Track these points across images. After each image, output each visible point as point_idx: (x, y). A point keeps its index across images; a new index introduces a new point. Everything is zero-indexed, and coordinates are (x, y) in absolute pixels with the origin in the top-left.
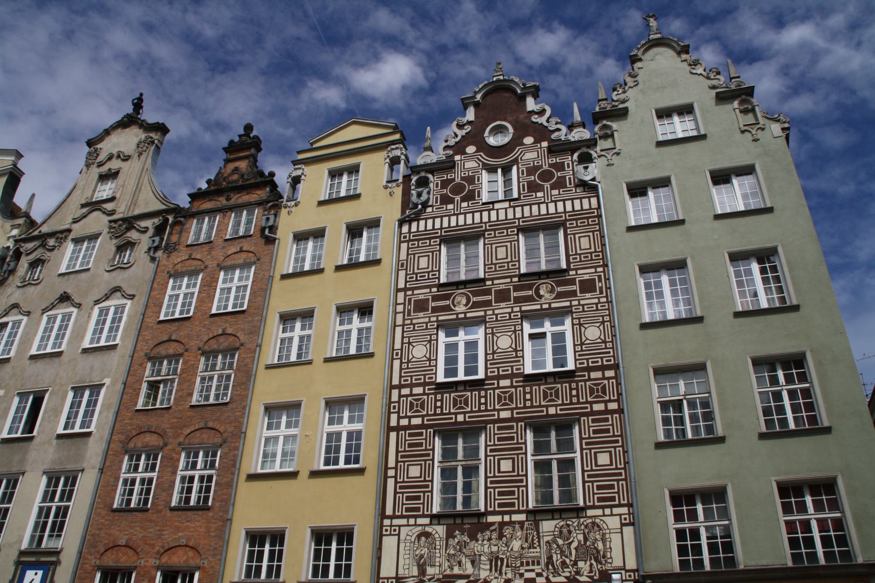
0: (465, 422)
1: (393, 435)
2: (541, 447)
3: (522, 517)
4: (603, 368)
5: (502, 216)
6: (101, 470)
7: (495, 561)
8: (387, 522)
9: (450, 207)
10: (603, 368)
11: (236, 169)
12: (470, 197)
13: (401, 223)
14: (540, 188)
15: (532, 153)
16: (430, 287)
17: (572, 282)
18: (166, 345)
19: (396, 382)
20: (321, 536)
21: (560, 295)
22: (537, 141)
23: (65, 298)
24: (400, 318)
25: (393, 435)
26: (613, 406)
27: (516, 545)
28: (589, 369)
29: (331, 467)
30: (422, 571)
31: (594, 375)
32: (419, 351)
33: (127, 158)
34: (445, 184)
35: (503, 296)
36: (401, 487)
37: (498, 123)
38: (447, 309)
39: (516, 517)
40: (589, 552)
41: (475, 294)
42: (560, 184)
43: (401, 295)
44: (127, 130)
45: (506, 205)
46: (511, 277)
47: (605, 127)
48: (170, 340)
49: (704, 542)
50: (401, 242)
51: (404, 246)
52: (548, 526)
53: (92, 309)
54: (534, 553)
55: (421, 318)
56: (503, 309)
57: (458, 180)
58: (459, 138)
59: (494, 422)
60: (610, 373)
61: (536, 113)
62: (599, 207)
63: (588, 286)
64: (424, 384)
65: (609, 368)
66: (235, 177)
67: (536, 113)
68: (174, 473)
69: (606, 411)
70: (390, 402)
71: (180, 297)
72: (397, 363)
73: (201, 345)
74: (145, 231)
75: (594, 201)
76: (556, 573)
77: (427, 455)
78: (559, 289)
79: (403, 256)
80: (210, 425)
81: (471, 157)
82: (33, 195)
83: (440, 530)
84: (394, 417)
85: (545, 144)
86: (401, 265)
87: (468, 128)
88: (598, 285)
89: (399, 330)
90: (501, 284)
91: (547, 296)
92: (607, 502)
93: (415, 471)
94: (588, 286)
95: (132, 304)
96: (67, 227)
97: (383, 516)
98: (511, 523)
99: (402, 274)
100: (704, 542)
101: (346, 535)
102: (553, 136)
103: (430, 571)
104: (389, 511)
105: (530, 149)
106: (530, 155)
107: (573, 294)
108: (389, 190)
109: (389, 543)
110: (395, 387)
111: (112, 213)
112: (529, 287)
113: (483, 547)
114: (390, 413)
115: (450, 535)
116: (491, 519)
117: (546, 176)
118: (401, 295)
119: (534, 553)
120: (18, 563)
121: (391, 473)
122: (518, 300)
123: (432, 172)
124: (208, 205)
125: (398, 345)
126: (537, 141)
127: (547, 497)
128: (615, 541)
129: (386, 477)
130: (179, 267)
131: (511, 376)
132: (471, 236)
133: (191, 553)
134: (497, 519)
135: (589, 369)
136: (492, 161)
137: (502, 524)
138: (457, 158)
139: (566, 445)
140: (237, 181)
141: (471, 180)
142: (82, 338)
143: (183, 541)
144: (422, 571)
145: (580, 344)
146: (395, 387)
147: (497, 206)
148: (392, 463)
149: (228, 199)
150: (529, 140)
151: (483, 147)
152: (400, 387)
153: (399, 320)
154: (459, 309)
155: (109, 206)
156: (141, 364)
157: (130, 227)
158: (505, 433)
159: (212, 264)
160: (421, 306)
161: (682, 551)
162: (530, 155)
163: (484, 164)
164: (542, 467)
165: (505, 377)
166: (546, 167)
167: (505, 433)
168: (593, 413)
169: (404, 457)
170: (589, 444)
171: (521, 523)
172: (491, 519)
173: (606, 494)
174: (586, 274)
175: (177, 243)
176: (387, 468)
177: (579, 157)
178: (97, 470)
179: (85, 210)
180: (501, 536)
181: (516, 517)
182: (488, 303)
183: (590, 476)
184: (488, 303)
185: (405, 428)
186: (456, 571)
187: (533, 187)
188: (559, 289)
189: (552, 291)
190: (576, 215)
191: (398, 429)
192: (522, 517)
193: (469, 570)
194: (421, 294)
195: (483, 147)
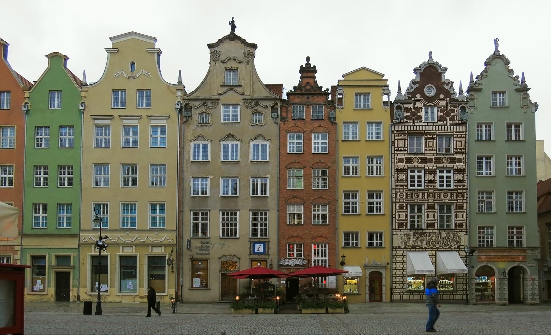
0: (418, 202)
1: (394, 204)
2: (441, 211)
3: (436, 231)
4: (462, 189)
5: (431, 129)
6: (278, 211)
7: (428, 242)
8: (394, 231)
9: (411, 121)
10: (462, 189)
11: (308, 83)
12: (418, 118)
13: (391, 125)
14: (445, 119)
15: (443, 103)
16: (404, 154)
17: (454, 158)
18: (294, 164)
19: (393, 187)
20: (370, 234)
21: (450, 163)
22: (445, 97)
23: (230, 136)
24: (393, 164)
25: (394, 204)
26: (464, 201)
27: (434, 238)
28: (458, 189)
29: (378, 213)
30: (406, 245)
31: (459, 191)
32: (401, 177)
33: (240, 62)
34: (408, 110)
35: (430, 160)
36: (398, 220)
37: (430, 85)
38: (410, 163)
39: (434, 231)
40: (454, 240)
41: (421, 158)
42: (453, 119)
43: (393, 155)
44: (233, 42)
45: (432, 124)
46: (434, 154)
47: (472, 95)
48: (295, 162)
49: (485, 239)
50: (391, 134)
51: (393, 135)
52: (443, 234)
53: (249, 143)
54: (439, 240)
55: (401, 165)
56: (431, 165)
57: (413, 110)
58: (414, 89)
59: (427, 203)
60: (464, 191)
61: (446, 83)
62: (466, 131)
63: (460, 161)
64: (404, 189)
65: (464, 189)
66: (309, 87)
67: (446, 83)
68: (311, 213)
69: (462, 202)
70: (392, 194)
71: (295, 143)
72: (393, 181)
73: (311, 165)
74: (266, 107)
75: (464, 128)
76: (445, 246)
77: (405, 211)
78: (450, 160)
79: (393, 140)
80: (322, 196)
81: (418, 100)
82: (180, 71)
83: (411, 234)
84: (394, 199)
85: (448, 99)
86: (392, 144)
87: (417, 85)
88: (463, 161)
89: (393, 169)
90: (430, 156)
91: (446, 162)
92: (461, 228)
93: (402, 216)
94: (460, 161)
95: (271, 144)
96: (216, 97)
97: (392, 229)
98: (432, 232)
99: (393, 147)
100: (485, 239)
101: (379, 234)
102: (452, 96)
103: (408, 244)
104: (394, 227)
105: (442, 100)
106: (442, 104)
107: (454, 163)
108: (385, 110)
109: (395, 237)
110: (393, 189)
111: (243, 94)
112: (440, 158)
113: (424, 238)
114: (392, 197)
115: (414, 235)
116: (426, 231)
117: (448, 114)
118: (393, 155)
119: (439, 240)
120: (250, 242)
121: (394, 216)
122: (436, 163)
123: (402, 104)
124: (297, 100)
125: (393, 174)
126: (445, 97)
127: (442, 225)
128: (462, 238)
129: (392, 218)
130: (291, 129)
131: (433, 189)
132: (418, 135)
133: (324, 239)
134: (429, 231)
135: (458, 189)
136: (427, 103)
137: (430, 233)
138: (413, 99)
139: (449, 211)
140: (310, 90)
141: (419, 110)
142: (248, 156)
143: (320, 235)
144: (406, 245)
145: (455, 180)
146: (393, 189)
147: (429, 124)
148: (394, 213)
149: (308, 98)
150: (442, 96)
151: (423, 96)
152: (395, 189)
153: (393, 165)
154: (416, 163)
155: (239, 89)
156: (285, 171)
157: (257, 104)
158: (431, 206)
159: (308, 131)
160: (401, 161)
161: (480, 241)
162: (442, 104)
163: (424, 105)
164: (442, 217)
165: (431, 189)
166: (448, 110)
167: (431, 206)
168: (458, 202)
169: (398, 212)
170: (456, 211)
171: (436, 232)
172: (426, 231)
173: (460, 226)
174: (459, 156)
175: (287, 117)
176: (392, 215)
177: (461, 108)
178: (276, 211)
179: (225, 89)
180: (429, 236)
181: (434, 231)
182: (425, 163)
183: (456, 221)
184: (425, 163)
185: (398, 203)
186: (416, 244)
187: (443, 118)
188: (450, 160)
189: (447, 161)
190: (458, 133)
191: (395, 202)
192: (436, 231)
193: (420, 244)
194: (401, 156)
195: (423, 96)
